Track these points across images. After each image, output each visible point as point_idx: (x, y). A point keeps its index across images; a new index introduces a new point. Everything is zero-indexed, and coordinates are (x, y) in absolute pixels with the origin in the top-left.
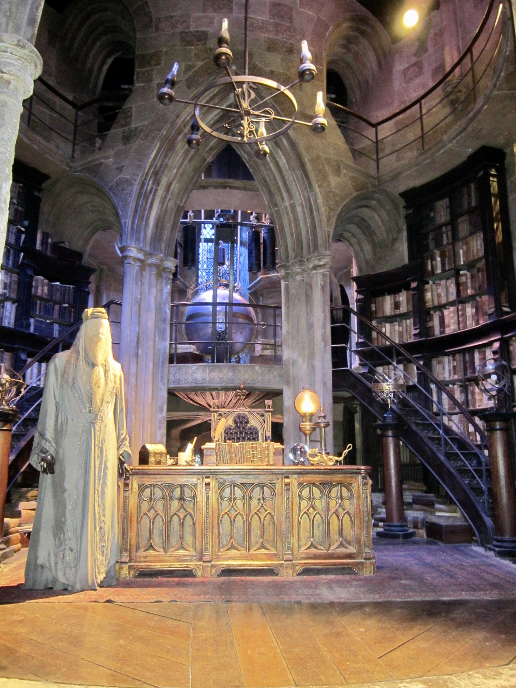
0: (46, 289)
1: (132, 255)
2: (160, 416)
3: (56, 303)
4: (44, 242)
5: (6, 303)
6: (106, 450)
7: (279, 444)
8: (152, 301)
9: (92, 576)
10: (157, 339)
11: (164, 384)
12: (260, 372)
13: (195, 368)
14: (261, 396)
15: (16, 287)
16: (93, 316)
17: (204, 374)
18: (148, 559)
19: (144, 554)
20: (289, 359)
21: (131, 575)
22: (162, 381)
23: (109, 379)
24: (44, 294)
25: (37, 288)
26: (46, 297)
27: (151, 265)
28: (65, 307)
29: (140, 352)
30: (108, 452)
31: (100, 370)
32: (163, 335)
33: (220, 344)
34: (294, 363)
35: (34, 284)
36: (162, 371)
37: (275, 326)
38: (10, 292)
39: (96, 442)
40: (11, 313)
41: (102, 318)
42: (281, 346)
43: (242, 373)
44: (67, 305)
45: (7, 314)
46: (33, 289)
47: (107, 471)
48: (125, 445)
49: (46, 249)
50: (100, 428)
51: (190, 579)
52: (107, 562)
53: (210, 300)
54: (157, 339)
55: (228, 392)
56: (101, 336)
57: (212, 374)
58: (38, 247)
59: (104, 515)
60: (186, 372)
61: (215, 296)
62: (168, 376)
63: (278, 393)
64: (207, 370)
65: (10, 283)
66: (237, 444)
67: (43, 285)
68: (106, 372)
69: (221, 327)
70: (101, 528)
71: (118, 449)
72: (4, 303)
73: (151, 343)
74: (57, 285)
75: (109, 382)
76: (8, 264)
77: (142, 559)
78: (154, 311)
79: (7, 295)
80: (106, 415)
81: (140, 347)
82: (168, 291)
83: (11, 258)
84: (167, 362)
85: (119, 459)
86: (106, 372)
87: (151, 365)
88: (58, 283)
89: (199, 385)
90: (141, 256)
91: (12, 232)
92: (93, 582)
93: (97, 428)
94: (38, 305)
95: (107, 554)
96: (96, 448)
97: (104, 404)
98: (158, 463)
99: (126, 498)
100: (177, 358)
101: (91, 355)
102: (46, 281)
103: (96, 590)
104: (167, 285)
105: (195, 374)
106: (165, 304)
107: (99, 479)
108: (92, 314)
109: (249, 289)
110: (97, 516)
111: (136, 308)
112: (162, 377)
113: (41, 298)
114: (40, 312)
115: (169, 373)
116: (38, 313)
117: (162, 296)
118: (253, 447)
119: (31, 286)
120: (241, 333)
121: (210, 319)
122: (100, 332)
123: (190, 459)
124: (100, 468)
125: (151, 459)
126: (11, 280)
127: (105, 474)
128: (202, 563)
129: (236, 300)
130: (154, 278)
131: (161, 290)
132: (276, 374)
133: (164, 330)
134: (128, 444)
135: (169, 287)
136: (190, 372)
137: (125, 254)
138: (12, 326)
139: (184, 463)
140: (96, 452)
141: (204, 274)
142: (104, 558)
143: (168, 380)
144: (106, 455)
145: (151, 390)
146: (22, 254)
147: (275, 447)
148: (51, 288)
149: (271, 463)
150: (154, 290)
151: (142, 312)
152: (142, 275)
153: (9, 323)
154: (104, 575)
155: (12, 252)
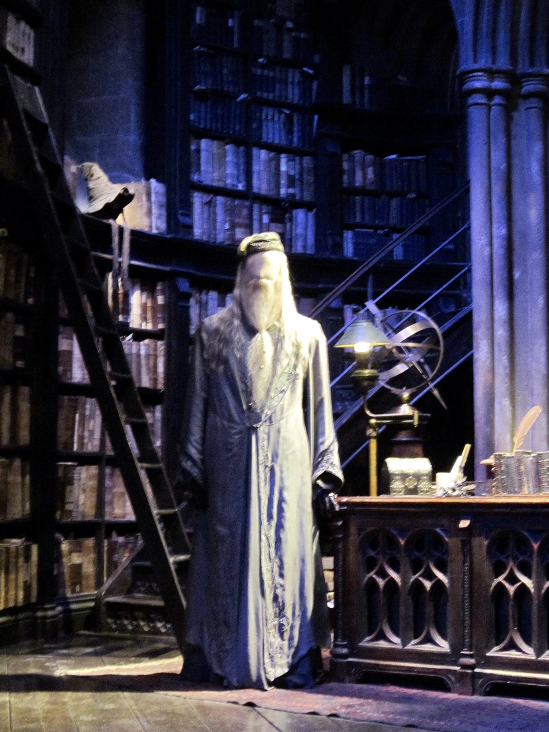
0: (370, 172)
1: (478, 85)
3: (392, 195)
4: (357, 87)
5: (294, 212)
6: (281, 472)
9: (258, 669)
15: (311, 179)
16: (252, 250)
19: (371, 645)
23: (283, 353)
24: (367, 181)
25: (352, 173)
26: (372, 188)
28: (413, 200)
29: (517, 275)
30: (285, 475)
31: (264, 340)
35: (345, 166)
38: (302, 192)
39: (261, 458)
40: (306, 228)
41: (264, 250)
44: (413, 196)
45: (300, 230)
46: (345, 178)
47: (284, 505)
48: (327, 461)
49: (362, 97)
50: (269, 434)
52: (293, 650)
56: (264, 281)
58: (346, 98)
59: (282, 575)
65: (301, 174)
67: (364, 169)
68: (278, 342)
70: (276, 598)
71: (315, 467)
72: (291, 213)
74: (391, 160)
75: (282, 356)
76: (291, 141)
79: (298, 197)
80: (278, 413)
83: (296, 129)
86: (278, 342)
88: (394, 156)
90: (498, 84)
91: (293, 83)
92: (259, 677)
94: (358, 205)
95: (291, 638)
96: (261, 468)
97: (272, 394)
99: (269, 552)
101: (249, 315)
102: (370, 158)
103: (266, 690)
107: (270, 517)
108: (249, 247)
110: (267, 577)
111: (498, 189)
113: (363, 192)
114: (363, 218)
116: (358, 220)
119: (342, 172)
124: (270, 500)
125: (396, 485)
126: (302, 168)
127: (281, 510)
128: (458, 668)
138: (310, 251)
140: (262, 475)
142: (286, 643)
144: (282, 479)
146: (316, 117)
148: (381, 169)
151: (516, 196)
153: (305, 247)
154: (286, 670)
155: (295, 118)
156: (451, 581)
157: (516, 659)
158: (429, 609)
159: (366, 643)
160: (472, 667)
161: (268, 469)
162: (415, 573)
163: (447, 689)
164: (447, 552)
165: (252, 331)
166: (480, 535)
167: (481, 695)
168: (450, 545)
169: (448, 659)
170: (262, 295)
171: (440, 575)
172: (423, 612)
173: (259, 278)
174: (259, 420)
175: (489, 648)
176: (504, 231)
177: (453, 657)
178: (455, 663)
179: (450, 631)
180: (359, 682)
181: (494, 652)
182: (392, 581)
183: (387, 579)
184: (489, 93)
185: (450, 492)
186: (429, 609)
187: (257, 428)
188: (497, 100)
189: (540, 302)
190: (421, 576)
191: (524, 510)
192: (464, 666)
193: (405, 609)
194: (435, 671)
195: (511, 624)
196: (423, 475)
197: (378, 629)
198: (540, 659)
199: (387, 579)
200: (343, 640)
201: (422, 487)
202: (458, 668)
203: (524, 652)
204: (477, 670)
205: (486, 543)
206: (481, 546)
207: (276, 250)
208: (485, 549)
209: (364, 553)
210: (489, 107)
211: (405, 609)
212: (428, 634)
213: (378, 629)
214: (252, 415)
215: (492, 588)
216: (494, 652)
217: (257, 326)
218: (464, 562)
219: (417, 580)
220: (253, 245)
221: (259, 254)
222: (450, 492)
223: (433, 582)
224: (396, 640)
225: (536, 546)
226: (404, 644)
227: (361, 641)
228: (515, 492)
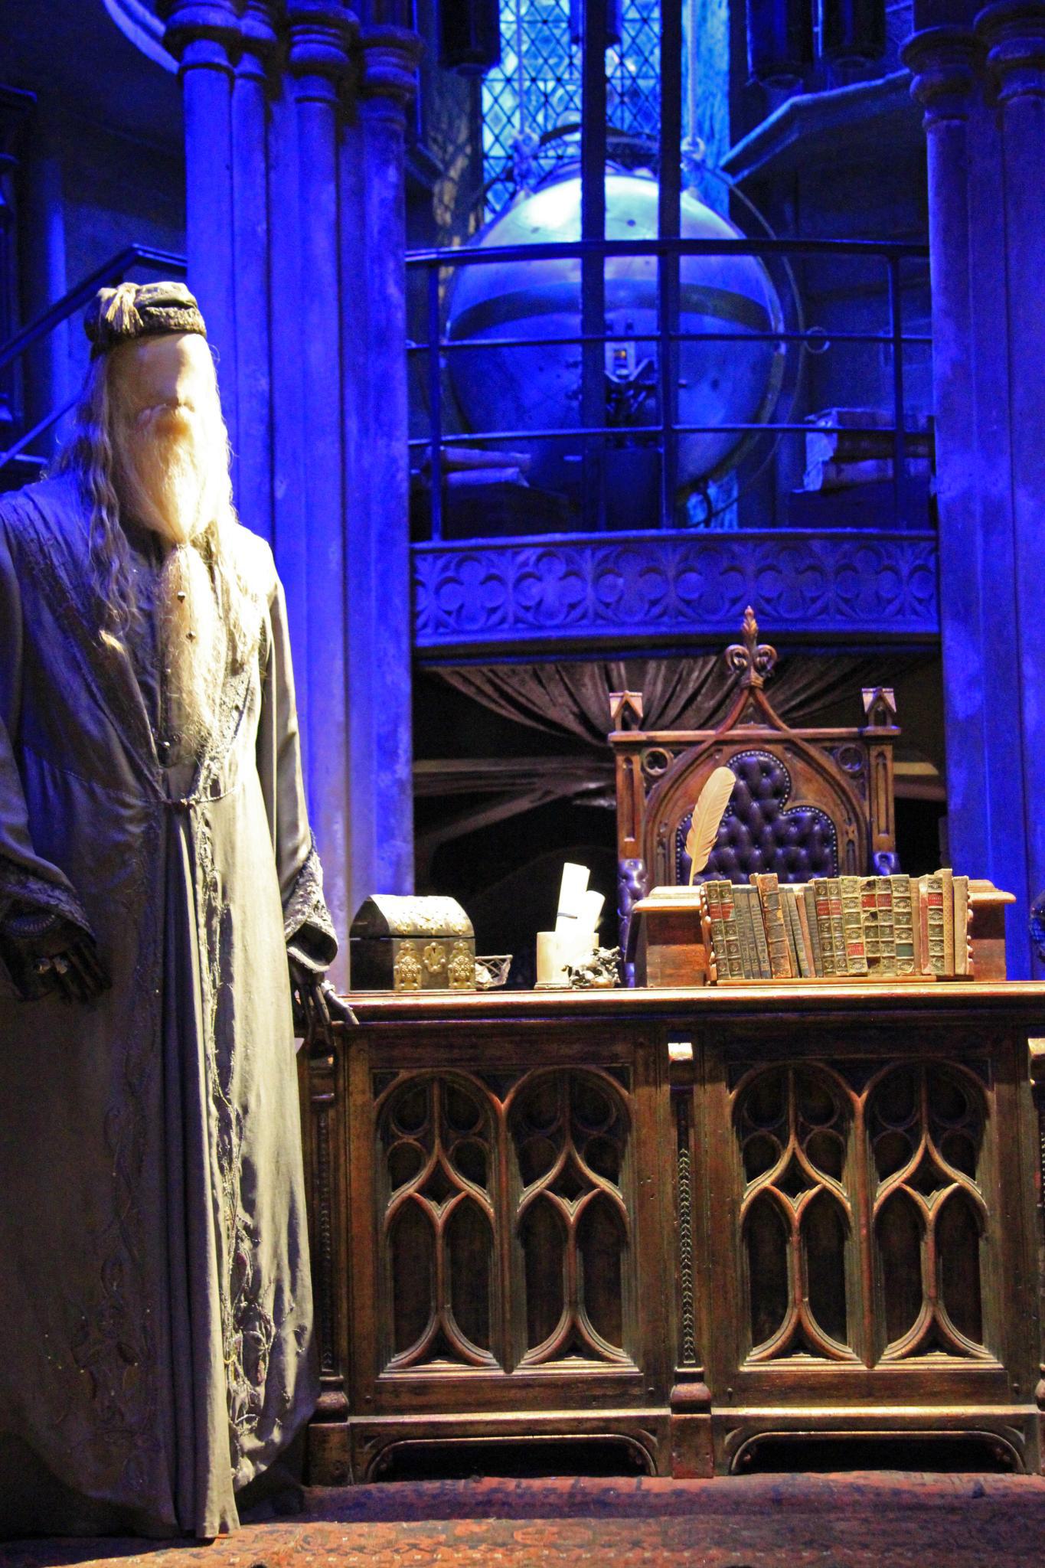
1: (216, 18)
2: (385, 779)
7: (988, 883)
8: (322, 243)
10: (353, 425)
11: (397, 634)
12: (830, 563)
13: (531, 555)
14: (830, 679)
17: (573, 580)
18: (432, 1399)
19: (413, 1375)
20: (966, 495)
21: (361, 1469)
22: (383, 617)
27: (302, 72)
32: (378, 408)
33: (619, 442)
34: (998, 515)
36: (383, 577)
37: (897, 341)
39: (199, 888)
41: (183, 331)
42: (928, 436)
43: (751, 569)
51: (622, 1483)
53: (572, 234)
54: (353, 425)
55: (684, 664)
57: (609, 579)
60: (490, 578)
61: (593, 206)
62: (413, 599)
63: (913, 664)
64: (588, 567)
66: (797, 888)
69: (623, 360)
73: (327, 448)
77: (406, 1399)
78: (331, 293)
81: (278, 467)
82: (389, 194)
84: (402, 535)
85: (292, 960)
87: (334, 553)
89: (554, 634)
93: (198, 827)
98: (440, 980)
100: (443, 511)
104: (386, 163)
105: (543, 576)
106: (380, 260)
109: (732, 168)
111: (250, 281)
112: (385, 601)
115: (415, 584)
117: (362, 218)
118: (870, 901)
120: (715, 385)
121: (576, 320)
122: (182, 396)
123: (590, 960)
128: (666, 1411)
129: (696, 225)
130: (320, 137)
131: (360, 195)
132: (905, 570)
133: (385, 378)
134: (318, 896)
135: (392, 174)
136: (511, 575)
137: (182, 15)
139: (565, 980)
141: (508, 101)
143: (414, 615)
145: (339, 664)
147: (975, 897)
149: (960, 971)
150: (327, 196)
152: (268, 121)
156: (642, 1196)
157: (817, 1375)
158: (572, 1266)
159: (396, 1370)
160: (703, 1406)
161: (216, 923)
162: (528, 1182)
163: (641, 1470)
164: (624, 1122)
165: (154, 546)
166: (714, 1079)
167: (731, 1473)
168: (635, 1106)
169: (636, 1391)
170: (181, 449)
171: (603, 1183)
172: (575, 1273)
173: (174, 403)
174: (191, 788)
175: (741, 1354)
176: (264, 384)
177: (654, 1383)
178: (658, 1398)
179: (634, 1322)
180: (381, 1476)
181: (754, 1362)
182: (468, 1207)
183: (452, 1202)
184: (237, 45)
185: (589, 975)
186: (572, 1266)
187: (190, 806)
188: (248, 65)
189: (331, 556)
190: (549, 1187)
191: (836, 1016)
192: (679, 1406)
193: (506, 1276)
194: (606, 1425)
195: (794, 1291)
196: (456, 936)
197: (429, 1333)
198: (877, 1368)
199: (452, 1202)
200: (335, 1368)
201: (458, 967)
202: (666, 1411)
203: (842, 1359)
204: (717, 1411)
205: (732, 1096)
206: (719, 1103)
207: (193, 331)
208: (728, 1111)
209: (387, 1138)
210: (232, 79)
211: (506, 1276)
212: (574, 1329)
213: (429, 1333)
214: (172, 772)
215: (743, 1207)
216: (754, 1362)
217: (168, 532)
218: (683, 1141)
219: (540, 1198)
220: (153, 310)
221: (168, 338)
222: (589, 975)
223: (585, 1199)
224: (488, 1357)
225: (860, 1101)
226: (507, 1361)
227: (380, 1368)
228: (761, 974)
